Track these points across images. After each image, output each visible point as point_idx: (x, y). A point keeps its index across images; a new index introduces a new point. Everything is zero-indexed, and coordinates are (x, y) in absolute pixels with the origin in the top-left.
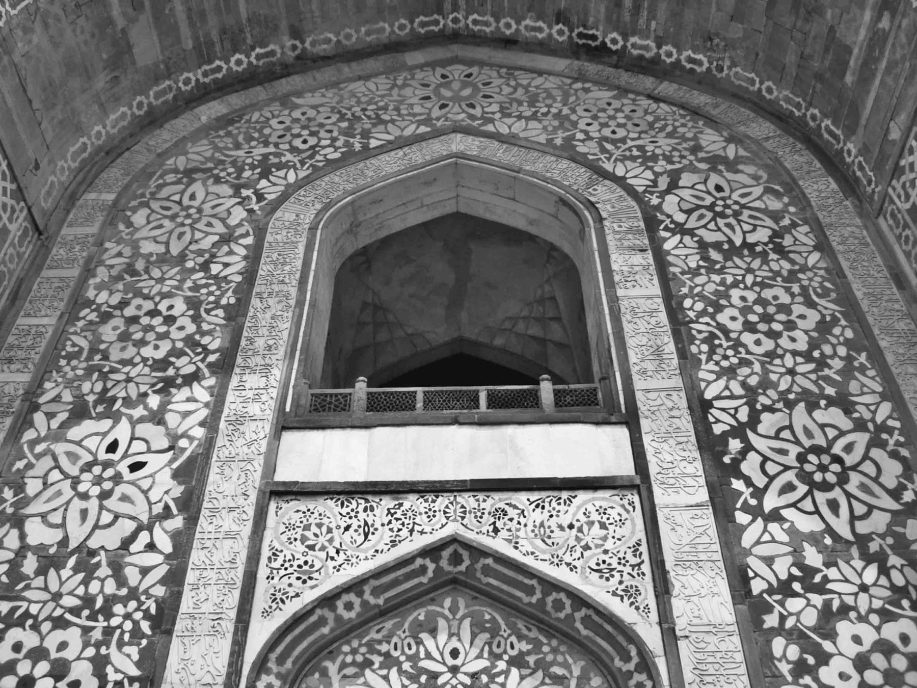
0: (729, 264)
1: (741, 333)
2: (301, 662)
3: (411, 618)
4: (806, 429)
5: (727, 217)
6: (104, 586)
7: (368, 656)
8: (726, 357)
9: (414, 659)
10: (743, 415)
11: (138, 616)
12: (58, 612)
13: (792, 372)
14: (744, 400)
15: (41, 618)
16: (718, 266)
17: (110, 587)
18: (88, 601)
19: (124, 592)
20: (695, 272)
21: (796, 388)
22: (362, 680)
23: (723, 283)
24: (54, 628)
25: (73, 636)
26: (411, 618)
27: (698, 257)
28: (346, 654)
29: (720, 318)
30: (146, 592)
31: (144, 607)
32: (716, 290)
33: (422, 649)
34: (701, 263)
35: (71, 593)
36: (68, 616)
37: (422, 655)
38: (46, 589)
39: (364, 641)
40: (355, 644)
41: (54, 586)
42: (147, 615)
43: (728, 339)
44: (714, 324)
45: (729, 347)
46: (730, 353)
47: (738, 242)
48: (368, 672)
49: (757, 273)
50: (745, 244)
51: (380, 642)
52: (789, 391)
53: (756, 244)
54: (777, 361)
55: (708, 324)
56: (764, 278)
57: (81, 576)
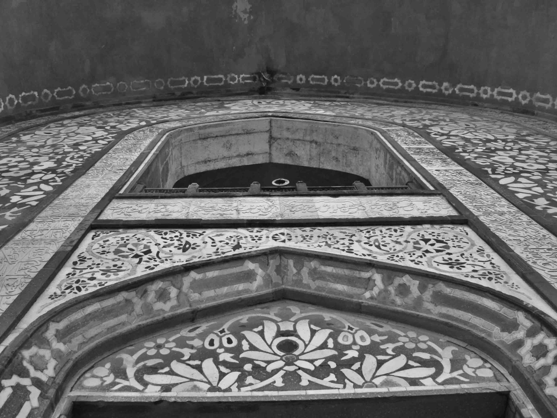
2: (92, 344)
40: (160, 341)
51: (192, 339)
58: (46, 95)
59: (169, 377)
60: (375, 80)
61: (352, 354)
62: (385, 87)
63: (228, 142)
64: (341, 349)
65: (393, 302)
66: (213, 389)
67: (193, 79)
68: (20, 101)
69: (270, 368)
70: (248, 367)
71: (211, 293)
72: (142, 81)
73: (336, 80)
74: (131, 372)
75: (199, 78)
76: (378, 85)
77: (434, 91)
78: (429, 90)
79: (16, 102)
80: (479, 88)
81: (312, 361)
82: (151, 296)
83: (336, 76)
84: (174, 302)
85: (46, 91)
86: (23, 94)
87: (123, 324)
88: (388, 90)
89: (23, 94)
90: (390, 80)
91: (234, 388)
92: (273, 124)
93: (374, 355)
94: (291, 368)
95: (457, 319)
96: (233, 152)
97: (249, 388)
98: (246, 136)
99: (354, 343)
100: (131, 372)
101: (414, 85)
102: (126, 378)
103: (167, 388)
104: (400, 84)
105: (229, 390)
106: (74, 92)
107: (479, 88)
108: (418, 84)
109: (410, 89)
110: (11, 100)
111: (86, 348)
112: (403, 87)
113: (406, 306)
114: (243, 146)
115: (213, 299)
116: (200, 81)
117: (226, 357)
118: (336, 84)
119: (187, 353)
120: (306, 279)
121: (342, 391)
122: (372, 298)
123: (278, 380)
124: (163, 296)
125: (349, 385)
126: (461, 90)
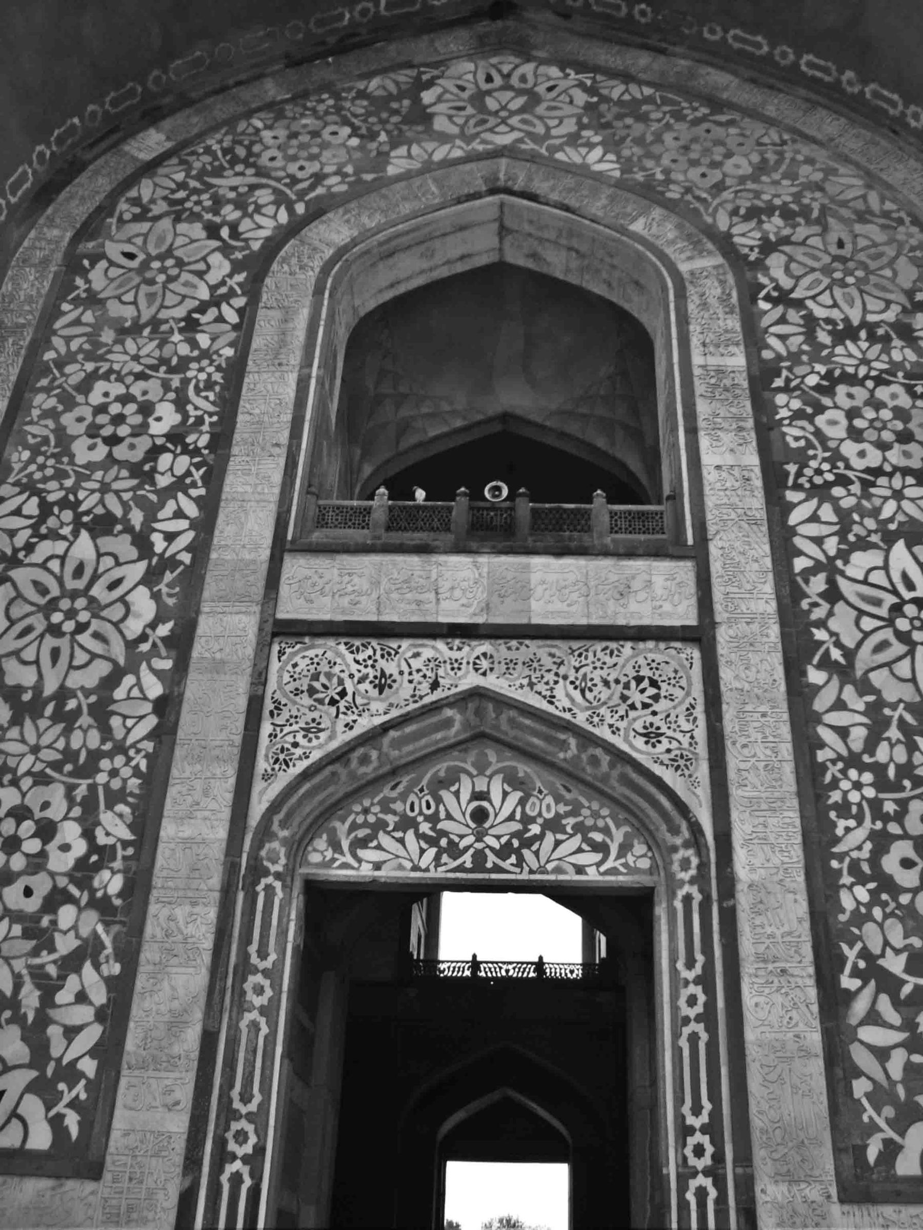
0: (839, 350)
1: (842, 440)
2: (309, 821)
3: (428, 776)
4: (905, 577)
5: (844, 285)
6: (86, 738)
7: (381, 816)
8: (819, 472)
9: (433, 819)
10: (832, 545)
11: (126, 772)
12: (39, 767)
13: (898, 495)
14: (837, 528)
15: (20, 773)
16: (825, 353)
17: (94, 739)
18: (69, 755)
19: (108, 746)
20: (795, 358)
21: (900, 518)
22: (374, 843)
23: (829, 375)
24: (35, 784)
25: (56, 794)
26: (428, 776)
27: (801, 338)
28: (357, 814)
29: (820, 420)
30: (133, 745)
31: (133, 763)
32: (818, 385)
33: (441, 808)
34: (805, 347)
35: (49, 747)
36: (48, 771)
37: (442, 815)
38: (23, 741)
39: (376, 800)
40: (367, 803)
41: (32, 739)
42: (137, 772)
43: (826, 449)
44: (811, 429)
45: (825, 460)
46: (826, 466)
47: (856, 322)
48: (381, 834)
49: (875, 364)
50: (864, 324)
51: (394, 800)
52: (891, 520)
53: (877, 324)
54: (882, 481)
55: (803, 428)
56: (882, 371)
57: (60, 727)
58: (93, 114)
59: (378, 852)
60: (718, 29)
61: (535, 829)
62: (737, 45)
63: (428, 249)
64: (527, 820)
65: (584, 770)
66: (415, 868)
67: (359, 7)
68: (54, 148)
69: (463, 844)
70: (444, 842)
71: (410, 748)
72: (261, 33)
73: (643, 13)
74: (345, 845)
75: (370, 5)
76: (724, 39)
77: (827, 79)
78: (818, 74)
79: (48, 153)
80: (906, 106)
81: (498, 837)
82: (354, 764)
83: (643, 6)
84: (375, 764)
85: (91, 108)
86: (56, 133)
87: (332, 794)
88: (740, 52)
89: (56, 133)
90: (748, 36)
91: (432, 868)
92: (506, 210)
93: (554, 833)
94: (479, 846)
95: (635, 804)
96: (438, 259)
97: (443, 868)
98: (459, 235)
99: (540, 814)
100: (345, 845)
101: (792, 57)
102: (342, 853)
103: (377, 866)
104: (766, 49)
105: (427, 870)
106: (140, 89)
107: (906, 106)
108: (799, 56)
109: (783, 63)
110: (41, 155)
111: (304, 827)
112: (770, 54)
113: (595, 777)
114: (453, 247)
115: (412, 753)
116: (373, 10)
117: (425, 828)
118: (643, 20)
119: (391, 819)
120: (505, 727)
121: (519, 877)
122: (565, 760)
123: (467, 859)
124: (365, 760)
125: (526, 869)
126: (876, 94)
